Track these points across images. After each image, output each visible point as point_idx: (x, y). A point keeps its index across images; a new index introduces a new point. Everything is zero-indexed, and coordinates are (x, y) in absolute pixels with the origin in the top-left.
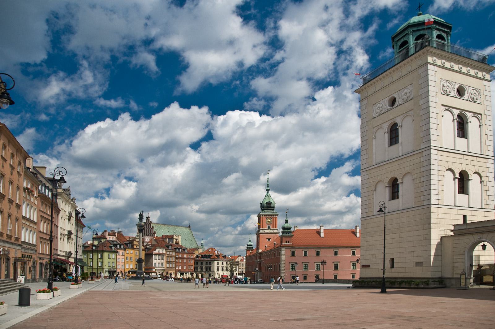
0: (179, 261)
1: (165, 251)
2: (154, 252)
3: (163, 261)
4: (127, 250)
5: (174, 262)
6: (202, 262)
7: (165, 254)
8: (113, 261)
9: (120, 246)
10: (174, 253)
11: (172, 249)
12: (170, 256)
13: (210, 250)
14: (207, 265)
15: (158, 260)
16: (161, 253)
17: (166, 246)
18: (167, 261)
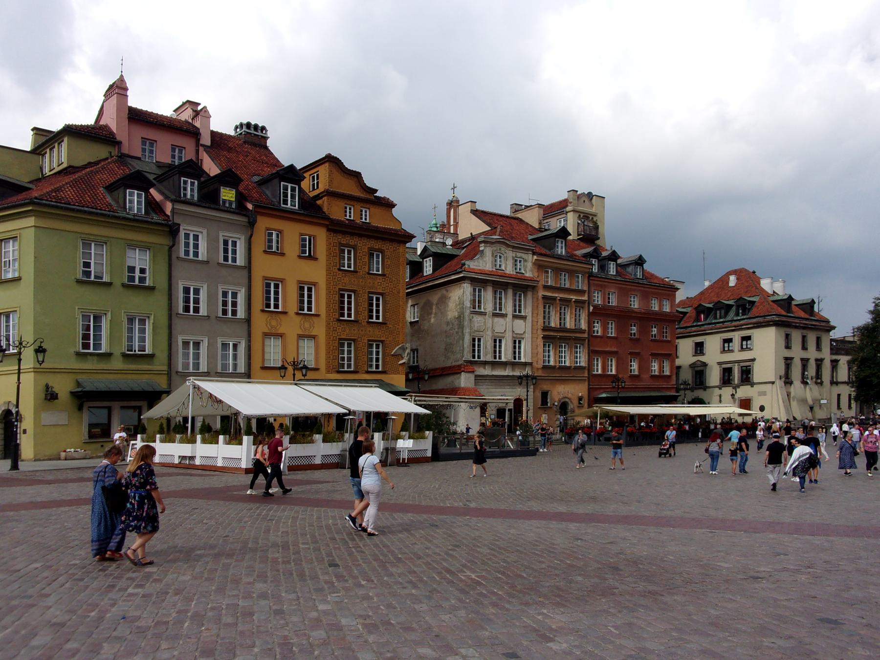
0: (605, 328)
1: (534, 264)
2: (472, 265)
3: (520, 326)
4: (263, 223)
5: (583, 332)
6: (699, 339)
7: (531, 280)
8: (137, 303)
9: (209, 196)
10: (581, 283)
11: (571, 257)
12: (561, 300)
13: (732, 281)
14: (732, 351)
15: (495, 315)
16: (510, 277)
17: (533, 240)
18: (546, 329)
